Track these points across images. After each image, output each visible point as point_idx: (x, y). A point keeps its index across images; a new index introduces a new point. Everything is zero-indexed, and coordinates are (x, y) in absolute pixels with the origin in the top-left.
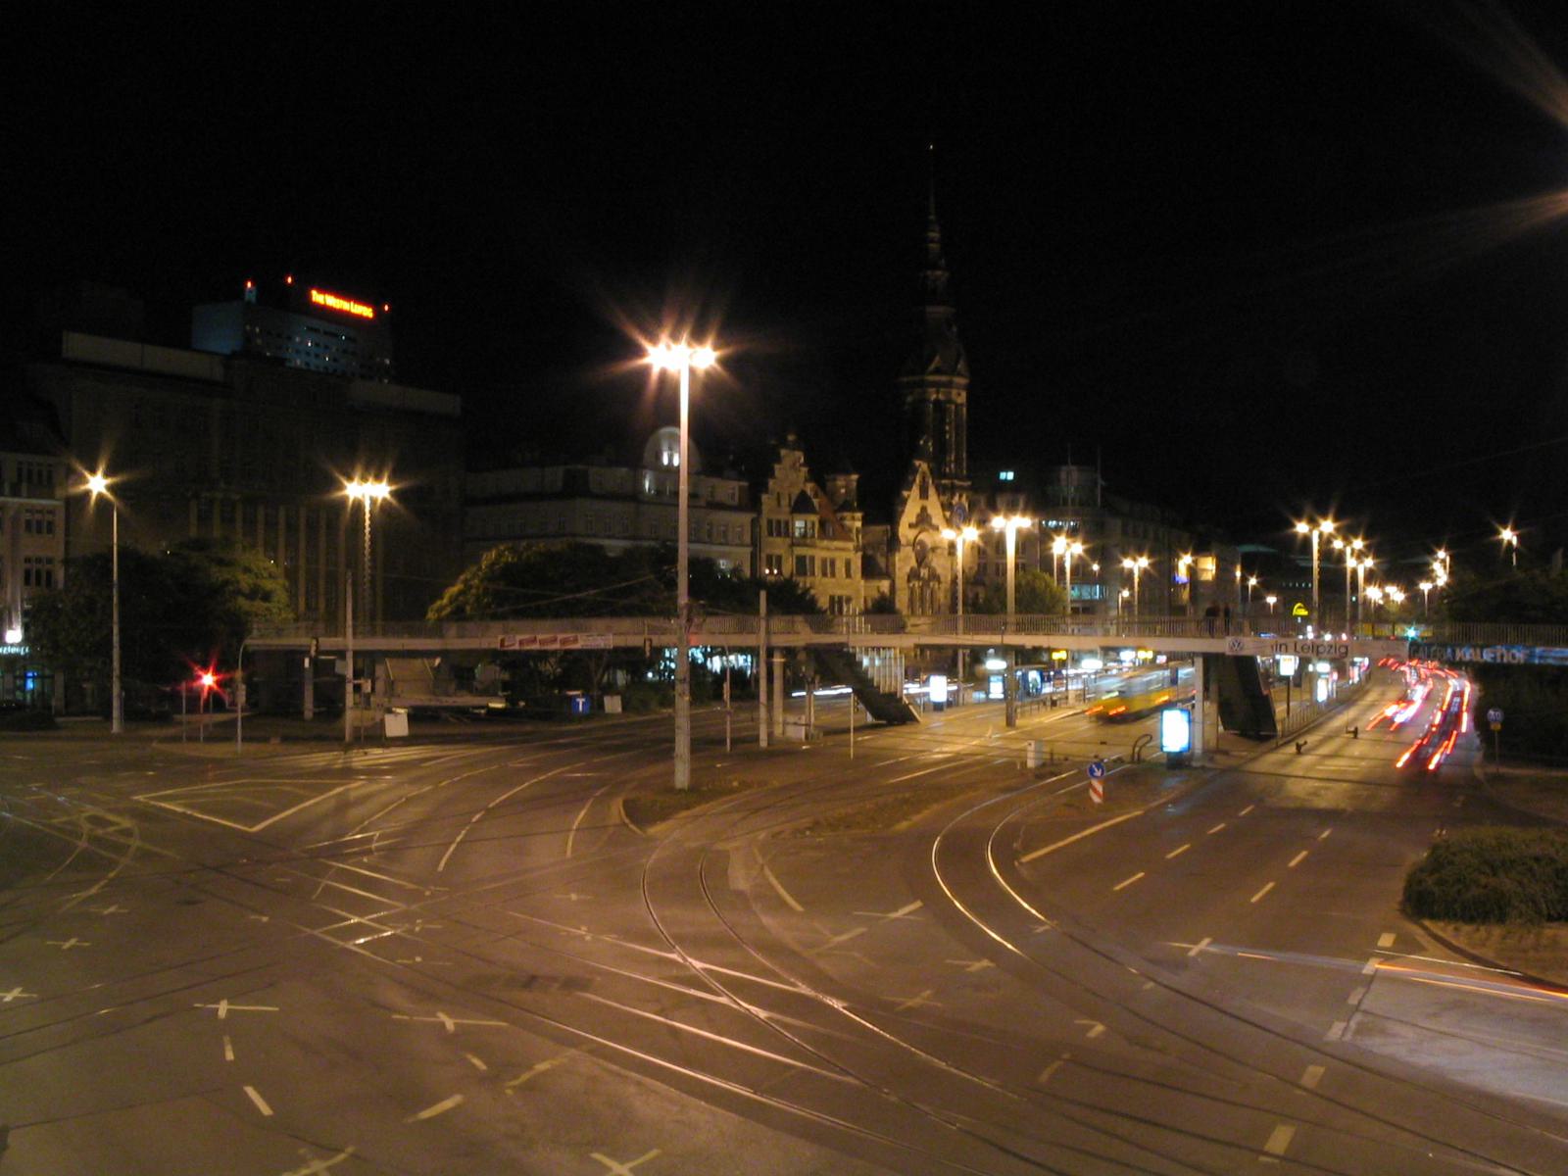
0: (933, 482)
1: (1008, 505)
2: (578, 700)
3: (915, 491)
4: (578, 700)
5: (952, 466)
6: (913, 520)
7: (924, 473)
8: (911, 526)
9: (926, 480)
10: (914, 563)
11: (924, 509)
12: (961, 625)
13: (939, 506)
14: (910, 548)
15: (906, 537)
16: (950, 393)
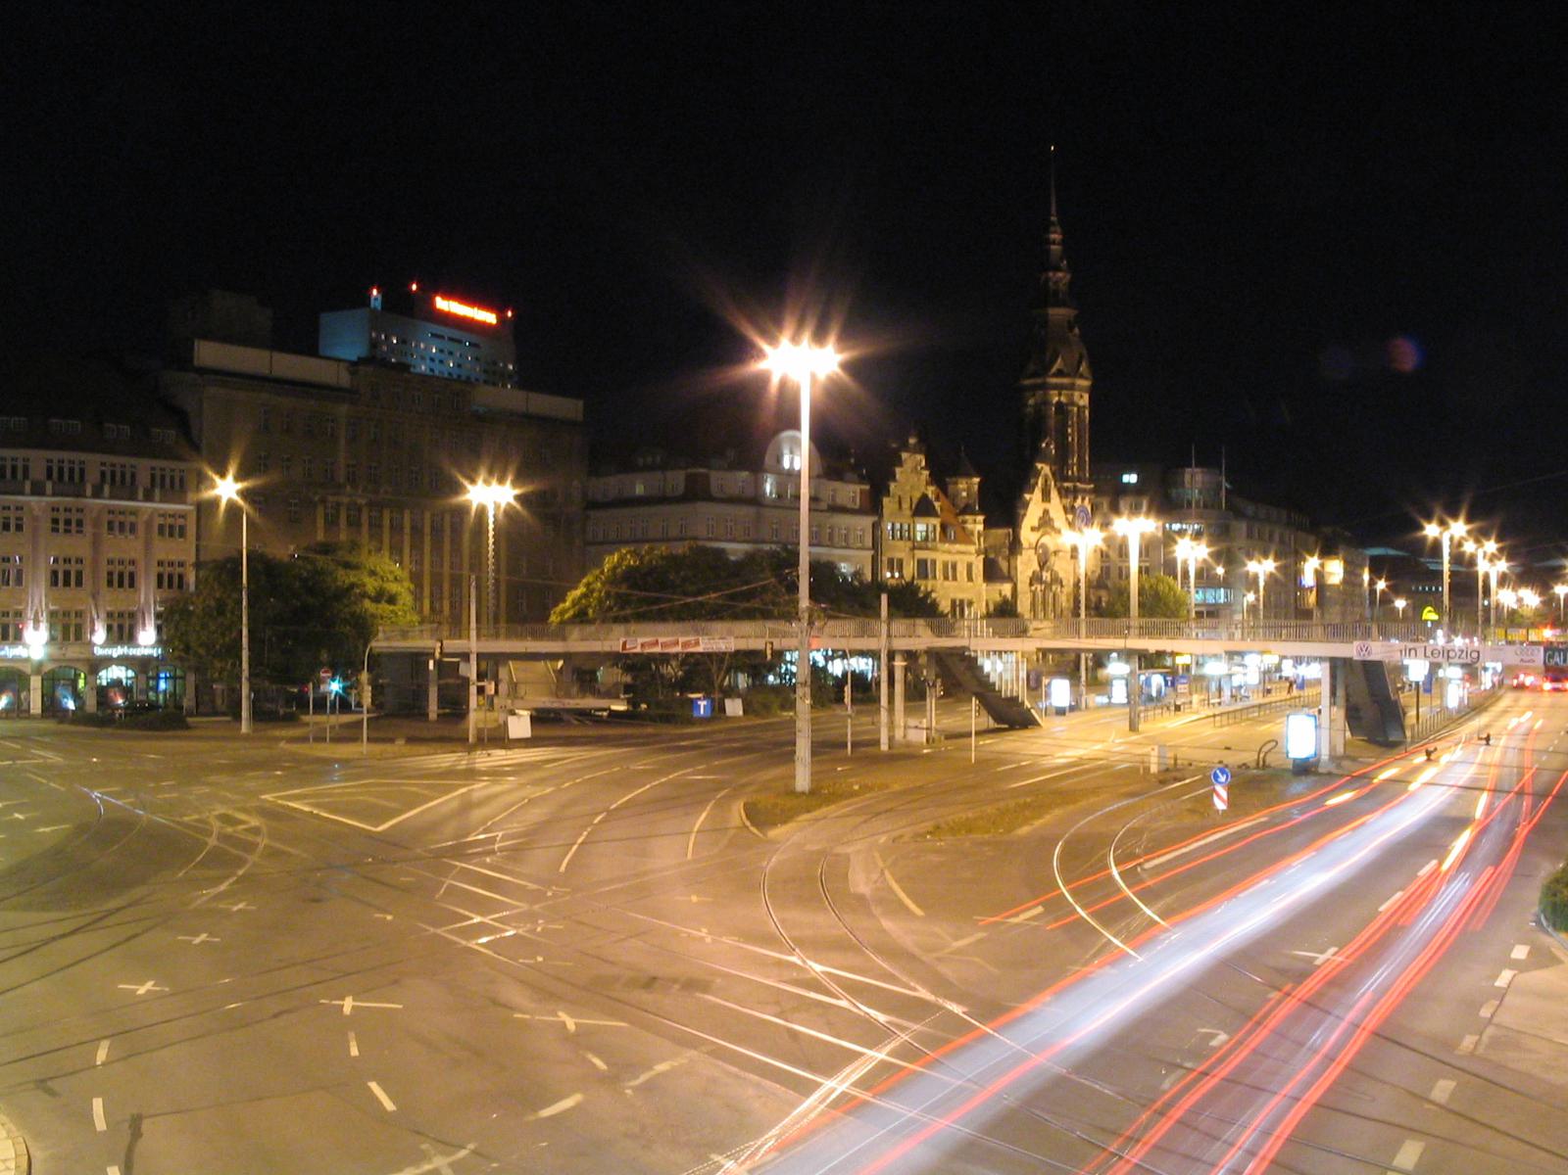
0: (1055, 485)
2: (699, 703)
3: (1037, 493)
4: (699, 703)
5: (1075, 469)
7: (1046, 476)
8: (1033, 529)
9: (1048, 483)
11: (1046, 512)
12: (503, 631)
14: (1033, 551)
16: (1072, 395)
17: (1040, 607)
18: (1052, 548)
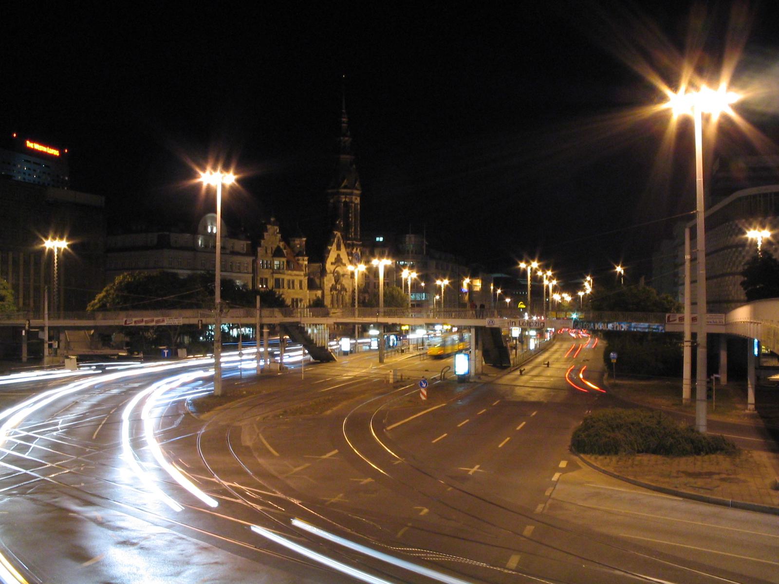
1: (380, 254)
2: (164, 351)
3: (334, 246)
4: (164, 351)
6: (333, 260)
7: (339, 237)
8: (332, 264)
10: (333, 282)
11: (338, 255)
13: (346, 253)
14: (332, 275)
15: (329, 269)
16: (352, 198)
17: (335, 302)
18: (341, 273)
